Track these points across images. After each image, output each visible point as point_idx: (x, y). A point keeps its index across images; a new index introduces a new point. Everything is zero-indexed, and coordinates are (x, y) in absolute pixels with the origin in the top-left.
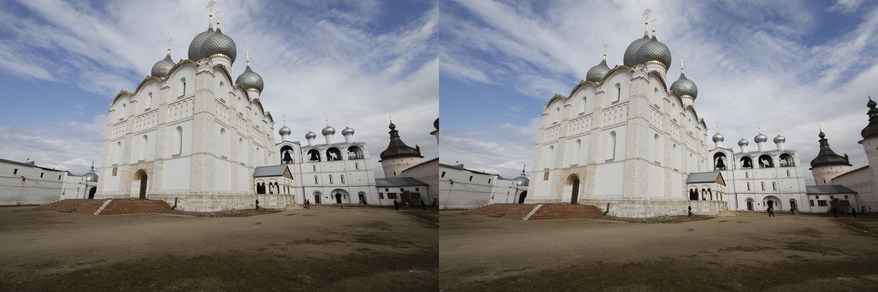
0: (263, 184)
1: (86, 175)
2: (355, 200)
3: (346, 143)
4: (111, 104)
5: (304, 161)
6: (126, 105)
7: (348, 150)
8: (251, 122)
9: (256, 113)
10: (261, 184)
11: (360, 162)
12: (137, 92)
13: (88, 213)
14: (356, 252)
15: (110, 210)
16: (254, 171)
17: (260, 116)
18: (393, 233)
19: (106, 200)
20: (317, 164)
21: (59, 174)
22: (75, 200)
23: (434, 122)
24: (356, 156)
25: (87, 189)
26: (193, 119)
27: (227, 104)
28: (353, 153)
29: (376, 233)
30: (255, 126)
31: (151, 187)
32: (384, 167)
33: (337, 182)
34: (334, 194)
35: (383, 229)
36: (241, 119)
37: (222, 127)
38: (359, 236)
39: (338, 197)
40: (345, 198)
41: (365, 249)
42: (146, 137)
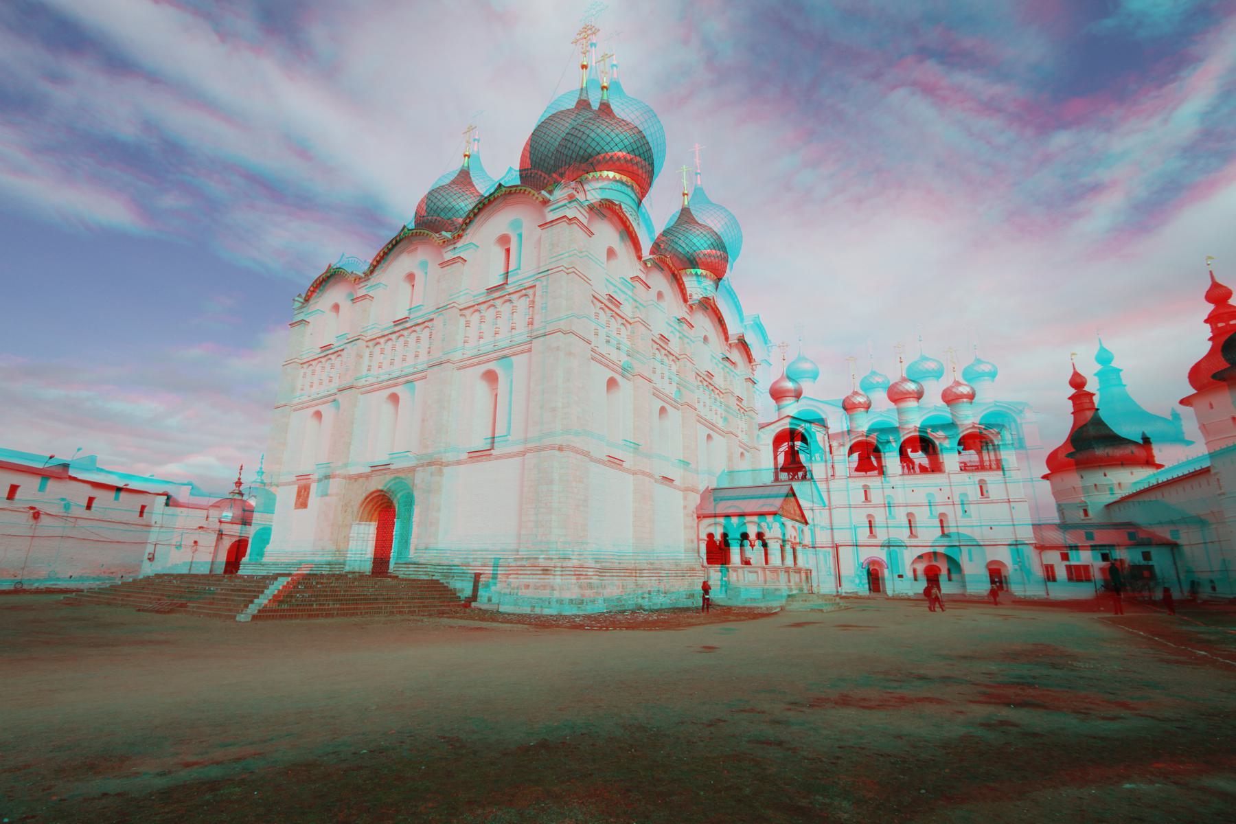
0: (725, 535)
1: (216, 506)
2: (980, 585)
3: (953, 425)
4: (297, 305)
5: (837, 473)
6: (341, 308)
7: (959, 444)
8: (690, 360)
9: (706, 339)
10: (718, 537)
11: (991, 477)
12: (372, 272)
13: (220, 616)
14: (979, 732)
15: (285, 606)
16: (698, 501)
17: (717, 346)
18: (1081, 678)
19: (276, 577)
20: (873, 481)
21: (140, 500)
22: (182, 576)
23: (1188, 370)
24: (982, 461)
25: (220, 547)
26: (530, 350)
27: (627, 310)
28: (972, 452)
29: (1034, 677)
30: (703, 374)
31: (405, 542)
32: (1056, 493)
33: (929, 536)
34: (921, 567)
35: (1054, 666)
36: (663, 352)
37: (610, 374)
38: (987, 686)
39: (932, 576)
40: (950, 579)
41: (1002, 723)
42: (394, 398)
